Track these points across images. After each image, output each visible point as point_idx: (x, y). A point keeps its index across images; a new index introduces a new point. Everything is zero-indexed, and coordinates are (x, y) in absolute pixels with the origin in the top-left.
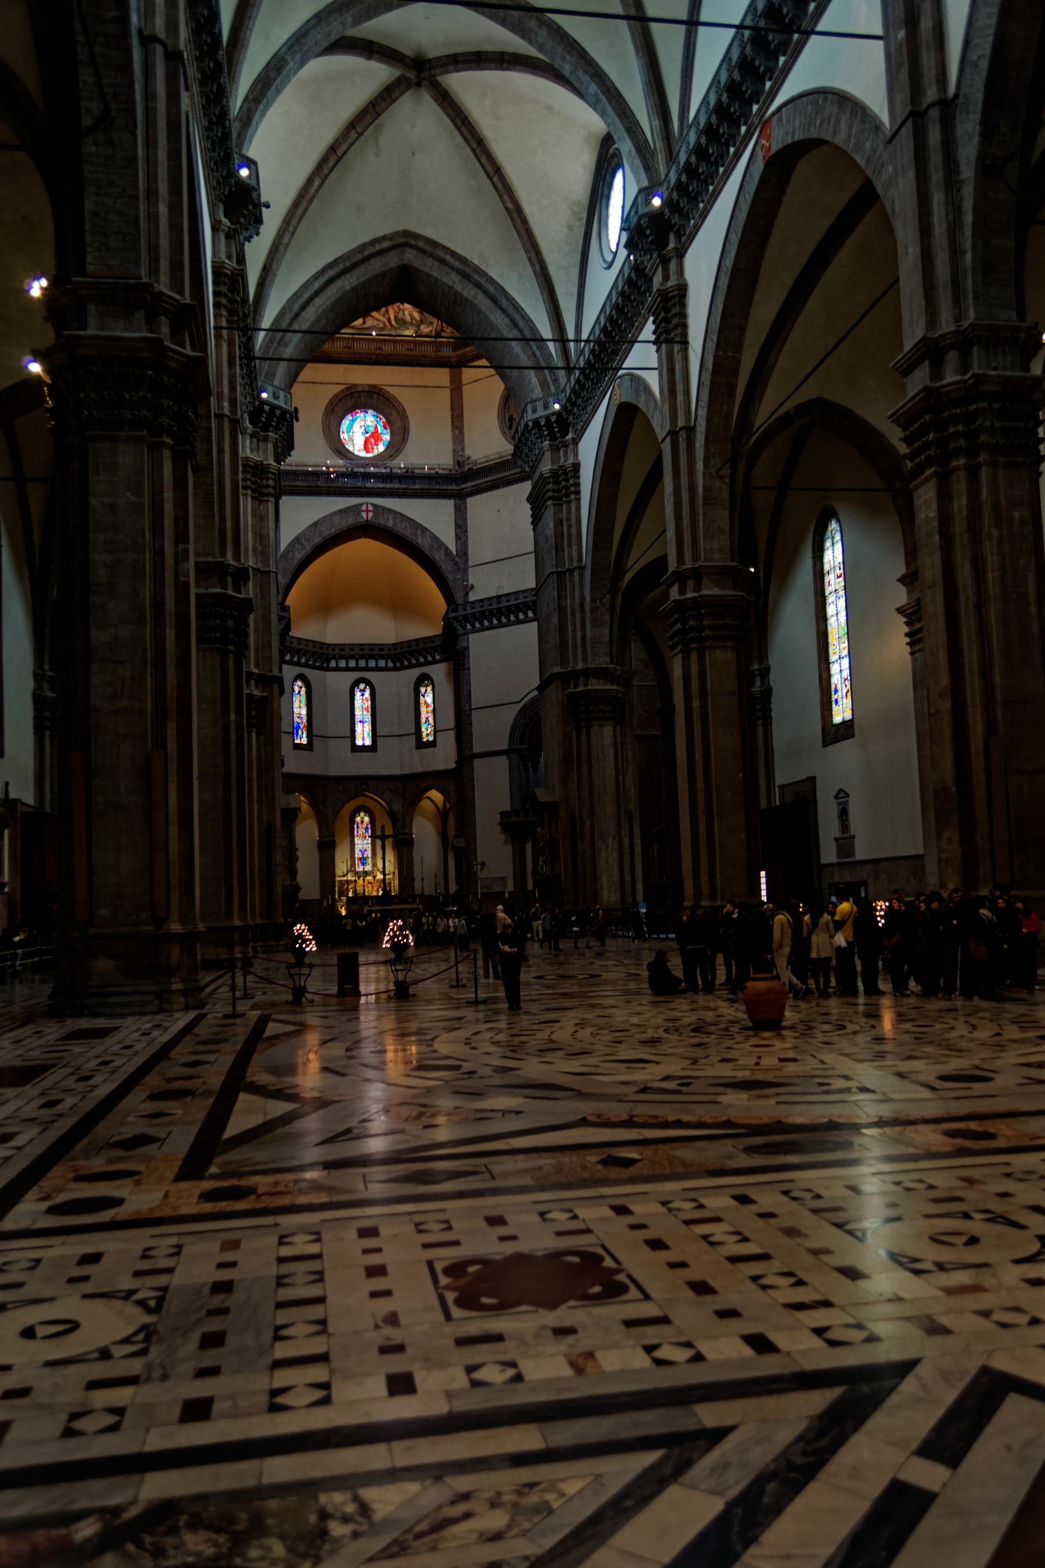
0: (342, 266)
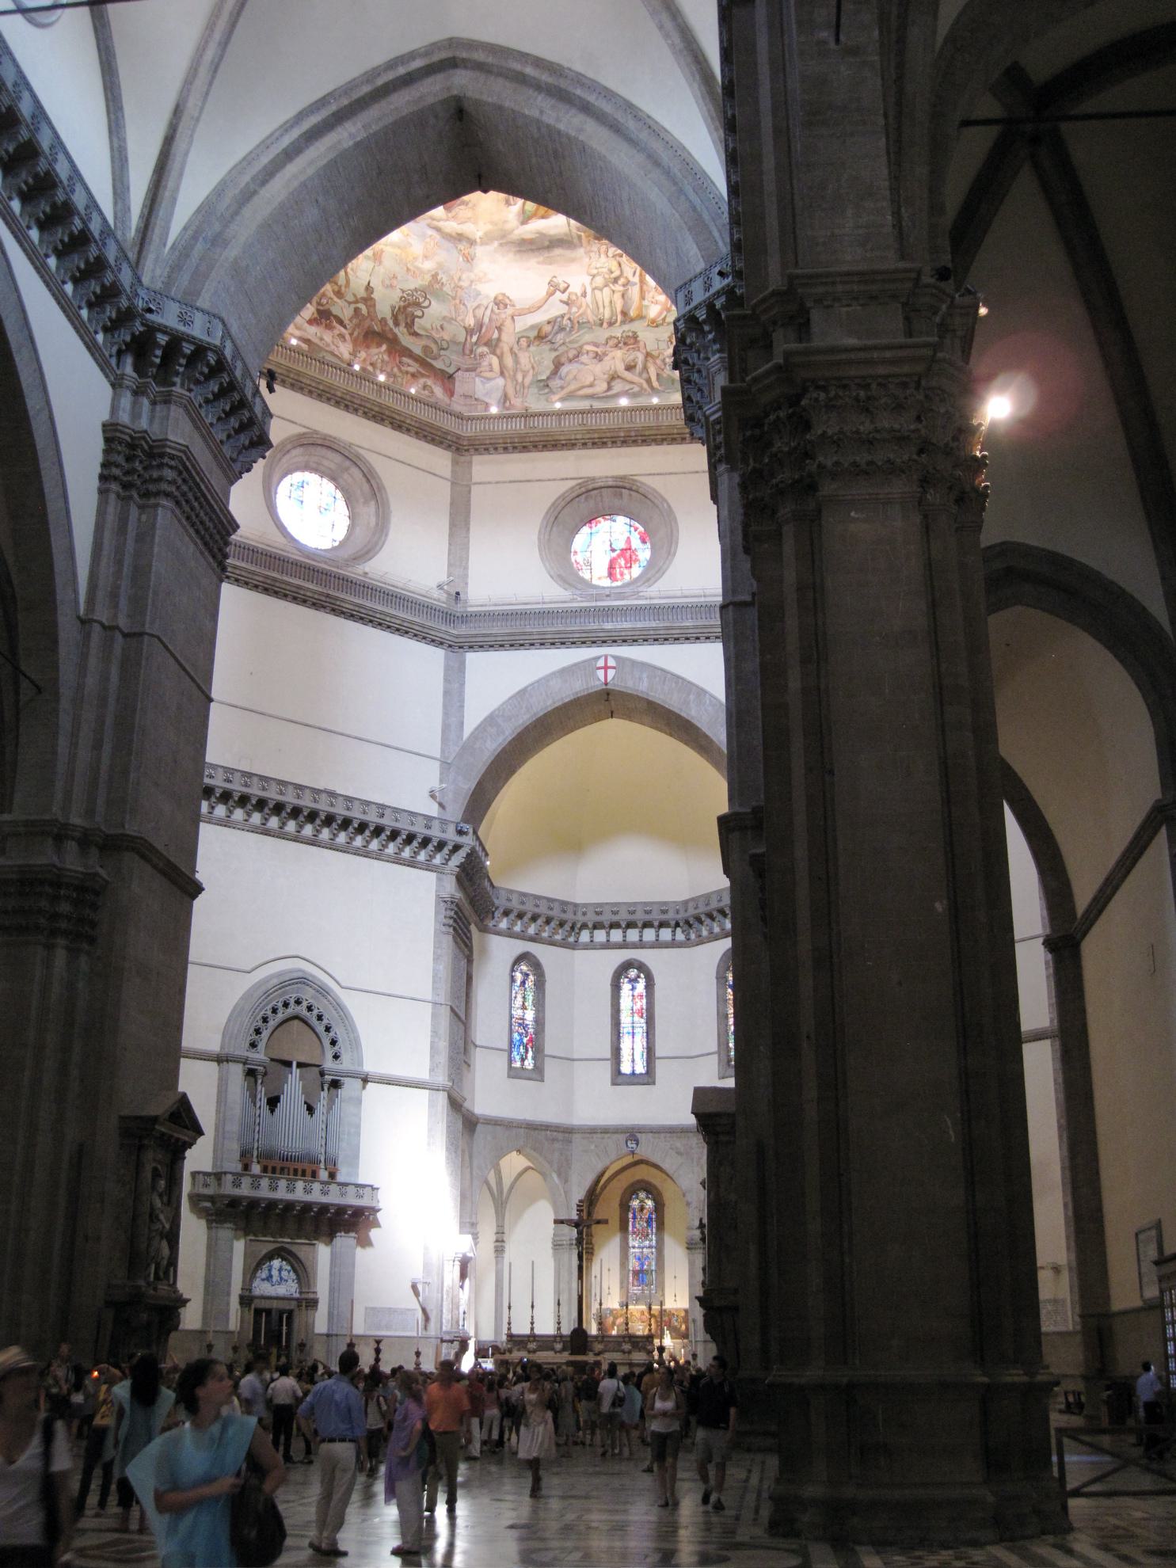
0: (333, 108)
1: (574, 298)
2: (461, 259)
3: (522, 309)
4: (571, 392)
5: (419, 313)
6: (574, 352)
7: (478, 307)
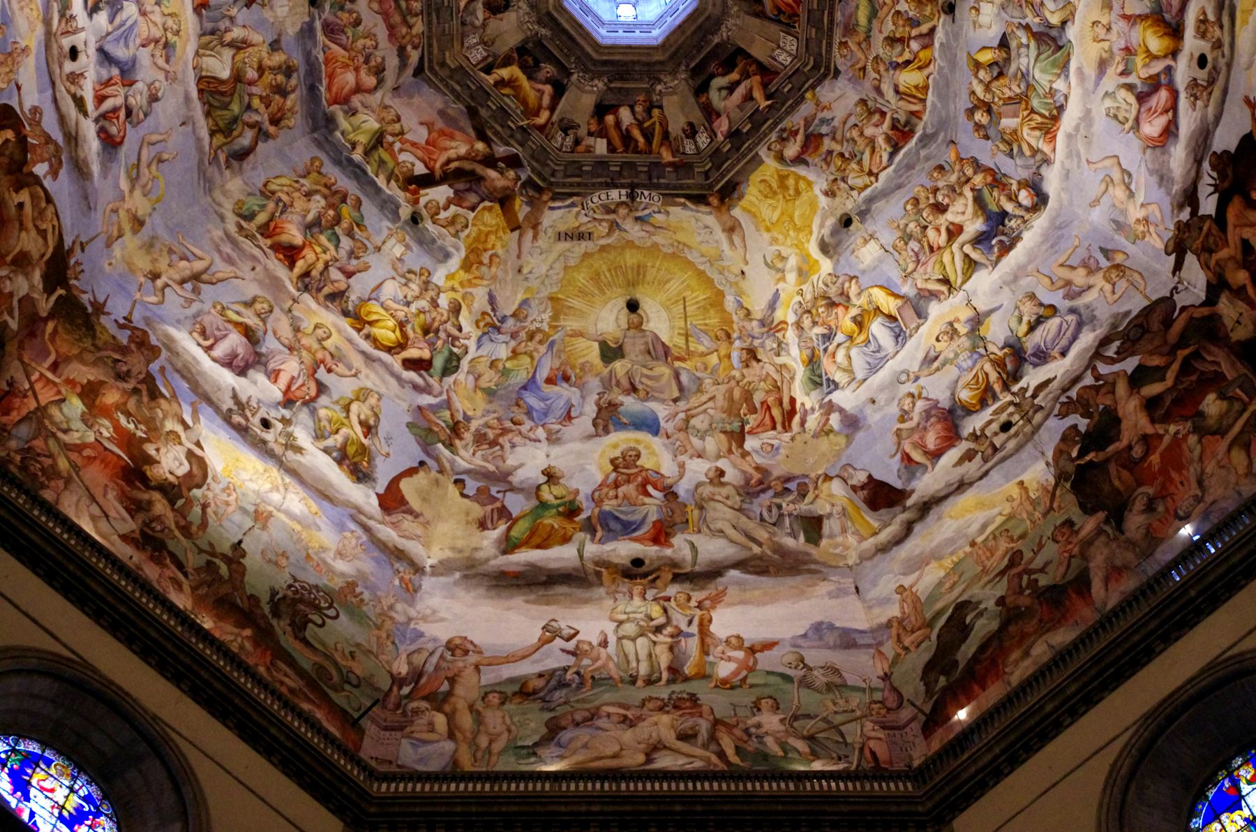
1: (586, 647)
2: (397, 582)
3: (494, 657)
4: (583, 763)
5: (319, 622)
6: (587, 714)
7: (419, 651)
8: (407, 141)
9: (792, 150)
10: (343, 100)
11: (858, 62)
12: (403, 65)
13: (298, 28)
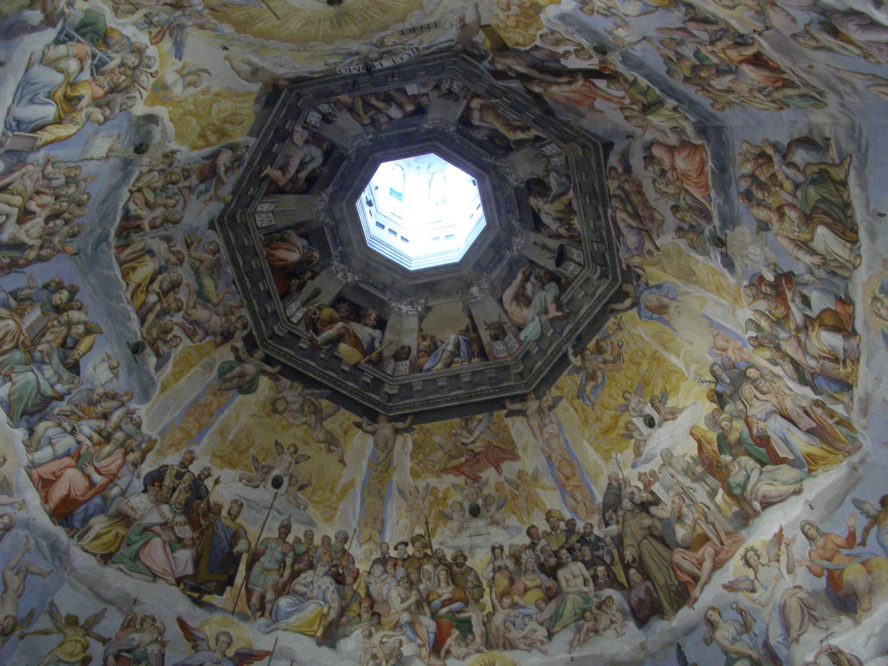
8: (617, 103)
9: (225, 158)
10: (685, 144)
11: (196, 248)
12: (625, 158)
13: (737, 229)
